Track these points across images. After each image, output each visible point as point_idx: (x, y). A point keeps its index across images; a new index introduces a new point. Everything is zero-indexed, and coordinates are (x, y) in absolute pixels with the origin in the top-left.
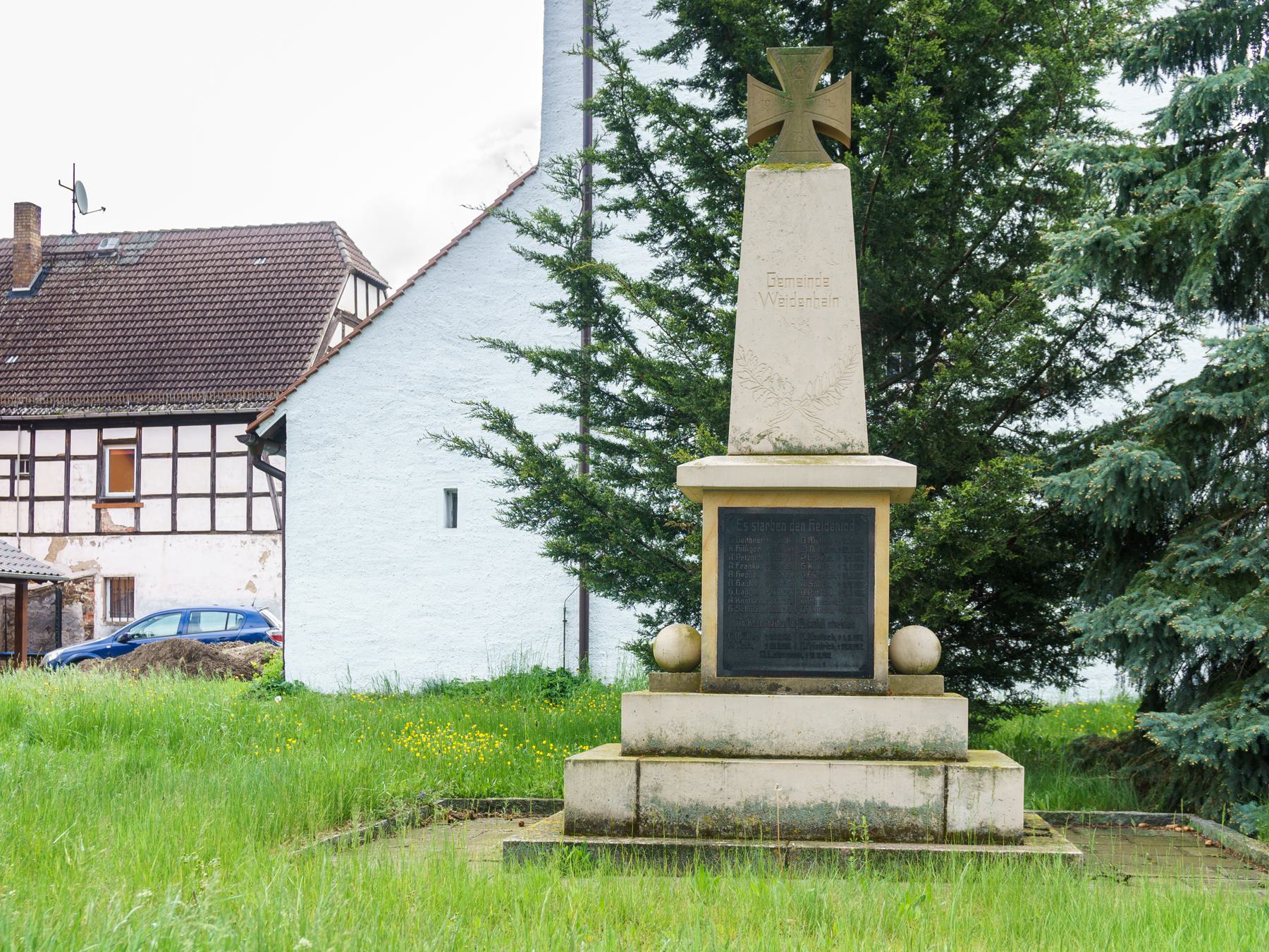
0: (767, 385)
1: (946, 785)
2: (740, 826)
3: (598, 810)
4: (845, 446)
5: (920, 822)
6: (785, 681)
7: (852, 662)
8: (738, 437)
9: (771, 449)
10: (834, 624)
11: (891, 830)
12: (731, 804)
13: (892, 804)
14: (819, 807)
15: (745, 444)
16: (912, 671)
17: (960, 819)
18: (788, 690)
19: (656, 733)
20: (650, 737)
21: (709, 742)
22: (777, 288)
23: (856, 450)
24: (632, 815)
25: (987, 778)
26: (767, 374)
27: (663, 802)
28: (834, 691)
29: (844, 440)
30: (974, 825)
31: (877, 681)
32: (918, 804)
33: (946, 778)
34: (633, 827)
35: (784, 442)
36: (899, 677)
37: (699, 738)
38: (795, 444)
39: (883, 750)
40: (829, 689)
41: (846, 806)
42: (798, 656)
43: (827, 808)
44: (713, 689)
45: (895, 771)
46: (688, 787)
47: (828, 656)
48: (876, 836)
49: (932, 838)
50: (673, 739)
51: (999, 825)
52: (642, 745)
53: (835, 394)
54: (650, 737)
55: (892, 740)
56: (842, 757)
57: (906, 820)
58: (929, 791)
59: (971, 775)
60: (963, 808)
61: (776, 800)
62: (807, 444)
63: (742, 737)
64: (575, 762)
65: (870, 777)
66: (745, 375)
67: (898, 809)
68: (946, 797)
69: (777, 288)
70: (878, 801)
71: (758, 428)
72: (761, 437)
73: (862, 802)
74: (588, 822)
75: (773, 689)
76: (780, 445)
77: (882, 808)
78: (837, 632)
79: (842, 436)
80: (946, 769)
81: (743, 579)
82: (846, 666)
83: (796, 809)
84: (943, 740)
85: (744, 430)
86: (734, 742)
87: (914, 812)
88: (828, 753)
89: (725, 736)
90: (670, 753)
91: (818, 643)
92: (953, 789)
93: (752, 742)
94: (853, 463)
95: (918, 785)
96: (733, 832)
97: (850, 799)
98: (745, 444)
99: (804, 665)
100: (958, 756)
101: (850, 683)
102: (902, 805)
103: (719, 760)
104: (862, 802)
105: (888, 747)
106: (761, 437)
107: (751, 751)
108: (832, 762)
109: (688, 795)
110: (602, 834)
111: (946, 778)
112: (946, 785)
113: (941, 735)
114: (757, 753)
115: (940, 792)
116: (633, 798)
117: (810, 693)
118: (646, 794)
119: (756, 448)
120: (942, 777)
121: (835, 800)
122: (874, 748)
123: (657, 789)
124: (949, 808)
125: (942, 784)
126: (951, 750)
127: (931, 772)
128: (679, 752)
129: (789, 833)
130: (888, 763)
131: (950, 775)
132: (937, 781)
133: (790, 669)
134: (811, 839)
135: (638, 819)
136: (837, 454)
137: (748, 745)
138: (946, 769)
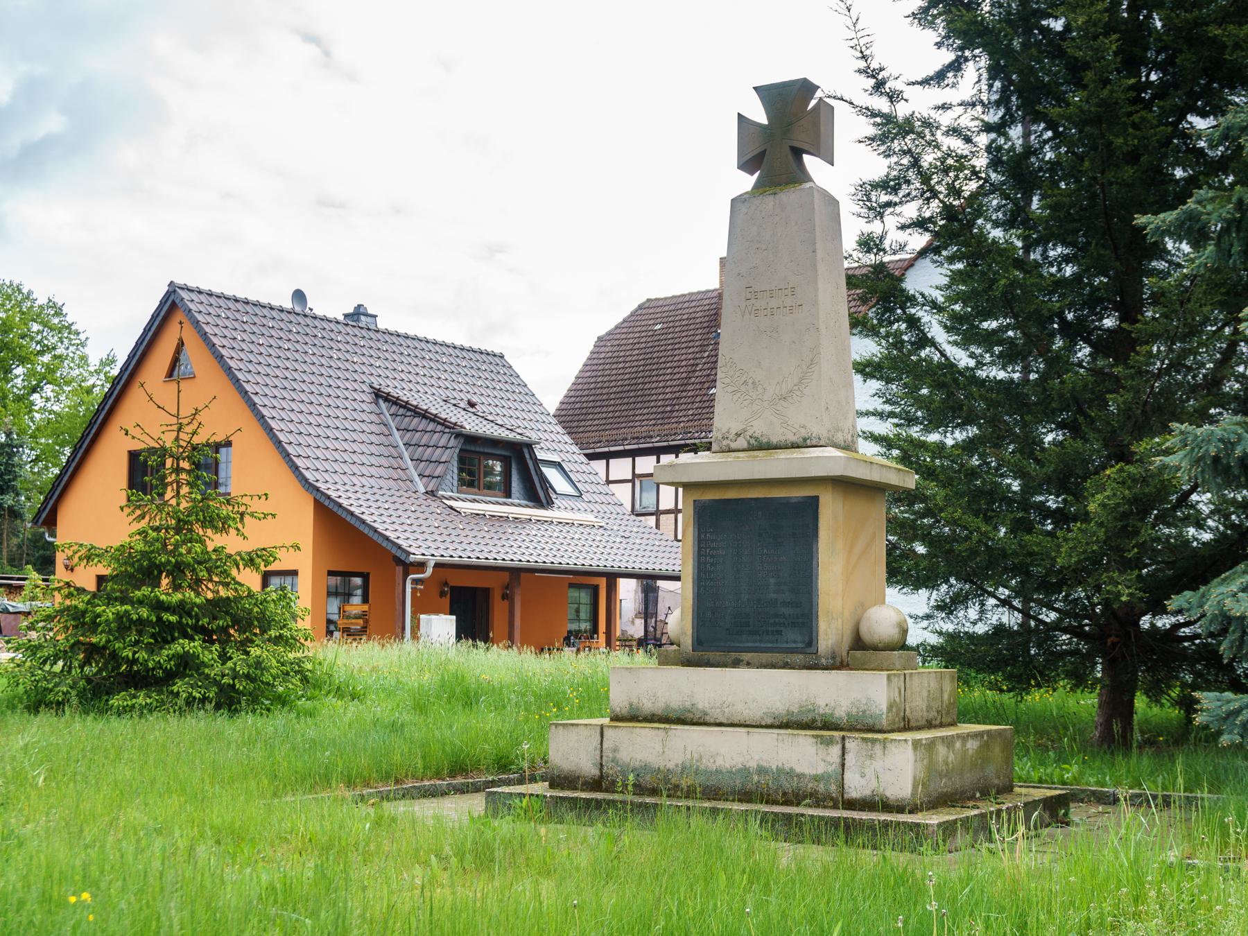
0: (743, 388)
1: (843, 754)
2: (678, 786)
3: (573, 768)
4: (805, 440)
5: (821, 788)
6: (746, 656)
7: (799, 638)
8: (720, 436)
9: (745, 445)
10: (786, 604)
11: (798, 794)
12: (671, 765)
13: (799, 770)
14: (739, 771)
15: (725, 442)
16: (875, 648)
17: (857, 786)
18: (749, 665)
19: (635, 701)
20: (631, 705)
21: (675, 710)
22: (753, 301)
23: (814, 442)
24: (597, 772)
25: (878, 747)
26: (743, 379)
27: (620, 762)
28: (786, 666)
29: (803, 433)
30: (867, 792)
31: (821, 657)
32: (820, 771)
33: (843, 748)
34: (596, 784)
35: (756, 439)
36: (858, 654)
37: (668, 706)
38: (765, 440)
39: (814, 721)
40: (781, 663)
41: (762, 771)
42: (756, 633)
43: (745, 771)
44: (689, 663)
45: (801, 739)
46: (643, 748)
47: (779, 632)
48: (639, 789)
49: (831, 804)
50: (648, 706)
51: (888, 794)
52: (625, 712)
53: (798, 393)
54: (631, 705)
55: (821, 711)
56: (780, 727)
57: (810, 785)
58: (829, 759)
59: (864, 746)
60: (858, 776)
61: (708, 764)
62: (774, 440)
63: (700, 706)
64: (557, 725)
65: (780, 744)
66: (727, 381)
67: (803, 775)
68: (843, 765)
69: (753, 301)
70: (787, 767)
71: (735, 427)
72: (738, 435)
73: (774, 767)
74: (566, 778)
75: (736, 664)
76: (752, 441)
77: (791, 774)
78: (788, 611)
79: (803, 430)
80: (843, 738)
81: (712, 564)
82: (795, 642)
83: (721, 772)
84: (864, 712)
85: (724, 430)
86: (694, 710)
87: (816, 778)
88: (769, 722)
89: (688, 704)
90: (652, 718)
91: (772, 621)
92: (849, 758)
93: (709, 711)
94: (795, 456)
95: (820, 752)
96: (674, 791)
97: (765, 764)
98: (725, 442)
99: (761, 641)
100: (877, 727)
101: (798, 658)
102: (807, 771)
103: (663, 726)
104: (774, 767)
105: (818, 718)
106: (738, 435)
107: (708, 719)
108: (750, 730)
109: (639, 757)
110: (575, 789)
111: (843, 748)
112: (843, 754)
113: (863, 707)
114: (712, 721)
115: (838, 760)
116: (598, 758)
117: (766, 666)
118: (608, 754)
119: (734, 445)
120: (840, 746)
121: (753, 765)
122: (806, 718)
123: (615, 750)
124: (845, 776)
125: (840, 753)
126: (871, 721)
127: (829, 742)
128: (652, 718)
129: (712, 793)
130: (796, 732)
131: (847, 745)
132: (835, 750)
133: (750, 645)
134: (781, 804)
135: (601, 776)
136: (798, 447)
137: (706, 714)
138: (843, 738)
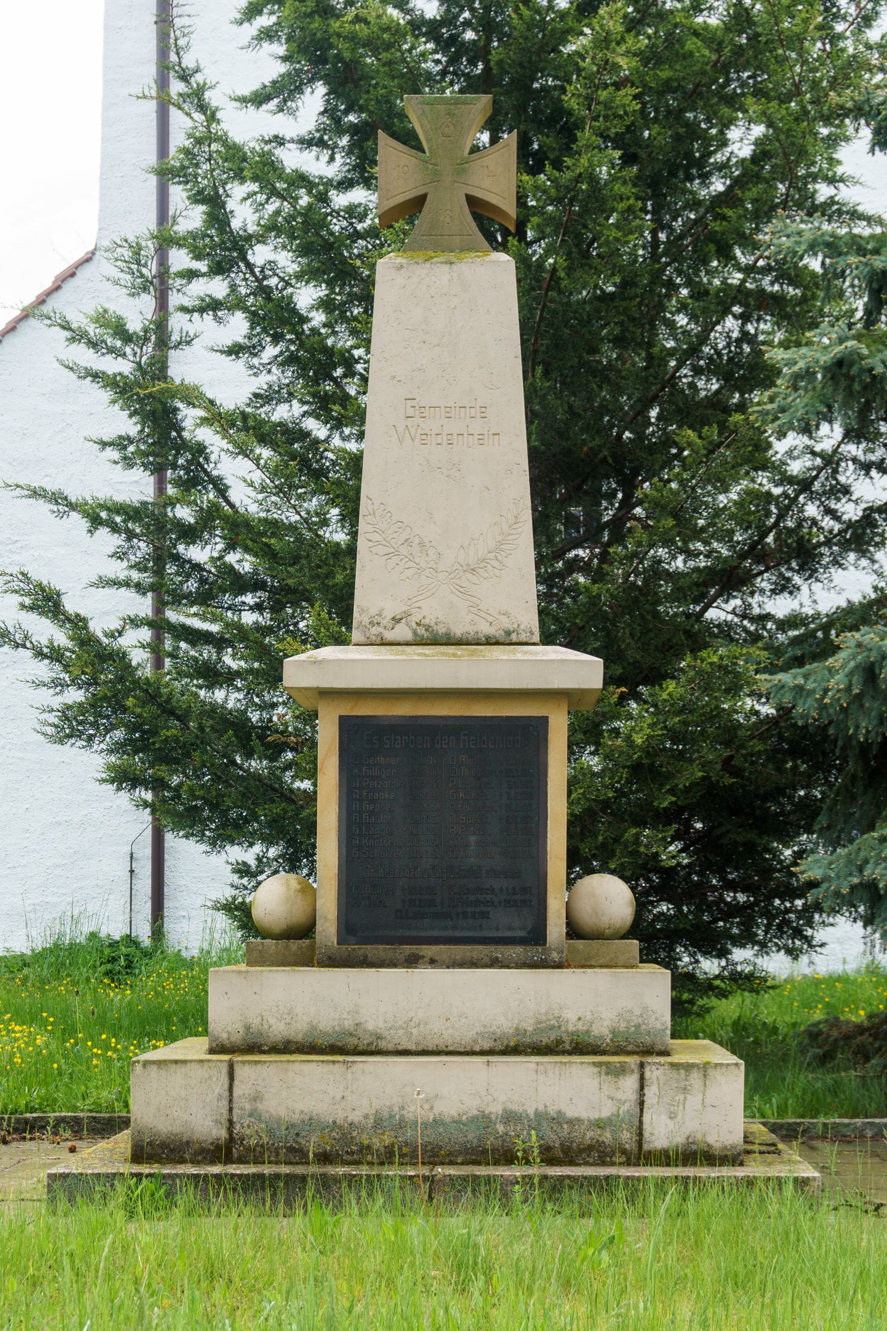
0: (404, 550)
1: (642, 1088)
2: (369, 1147)
3: (177, 1128)
4: (508, 633)
5: (607, 1137)
8: (366, 620)
11: (570, 1148)
12: (356, 1117)
13: (571, 1112)
14: (473, 1120)
15: (375, 630)
16: (597, 935)
17: (661, 1132)
18: (433, 962)
19: (255, 1022)
20: (248, 1028)
21: (326, 1034)
22: (417, 420)
23: (523, 638)
24: (223, 1134)
25: (695, 1075)
28: (494, 963)
30: (680, 1140)
31: (550, 949)
32: (605, 1113)
33: (642, 1078)
34: (223, 1151)
35: (428, 628)
36: (580, 944)
37: (313, 1028)
38: (441, 630)
39: (559, 1042)
40: (486, 960)
41: (510, 1117)
43: (484, 1120)
44: (333, 962)
45: (575, 1070)
46: (300, 1095)
47: (485, 915)
48: (549, 1158)
49: (623, 1159)
51: (711, 1140)
52: (237, 1039)
53: (495, 563)
54: (248, 1028)
55: (571, 1028)
57: (589, 1134)
59: (674, 1074)
60: (664, 1118)
61: (417, 1111)
62: (458, 631)
63: (370, 1026)
64: (146, 1063)
65: (542, 1078)
66: (376, 537)
67: (579, 1120)
68: (642, 1103)
69: (417, 420)
70: (552, 1110)
71: (392, 609)
72: (396, 620)
73: (531, 1112)
74: (164, 1145)
75: (412, 962)
76: (421, 631)
77: (558, 1119)
80: (642, 1065)
82: (510, 928)
84: (638, 1026)
85: (373, 611)
86: (360, 1033)
87: (599, 1124)
88: (486, 1046)
89: (349, 1024)
90: (275, 1049)
91: (472, 898)
92: (651, 1093)
93: (385, 1033)
94: (519, 656)
95: (605, 1087)
96: (359, 1154)
97: (515, 1107)
98: (375, 630)
99: (454, 928)
102: (584, 1115)
103: (340, 1058)
104: (531, 1112)
105: (565, 1038)
106: (396, 620)
107: (383, 1045)
109: (299, 1106)
110: (182, 1161)
111: (642, 1078)
112: (642, 1088)
113: (636, 1021)
114: (391, 1047)
116: (225, 1111)
117: (462, 965)
118: (242, 1105)
119: (389, 636)
120: (636, 1077)
121: (496, 1109)
122: (546, 1039)
123: (256, 1098)
124: (646, 1118)
126: (648, 1040)
129: (434, 1155)
130: (565, 1059)
131: (648, 1074)
132: (630, 1083)
133: (435, 933)
134: (462, 1163)
135: (231, 1139)
136: (497, 643)
137: (379, 1037)
138: (642, 1065)
